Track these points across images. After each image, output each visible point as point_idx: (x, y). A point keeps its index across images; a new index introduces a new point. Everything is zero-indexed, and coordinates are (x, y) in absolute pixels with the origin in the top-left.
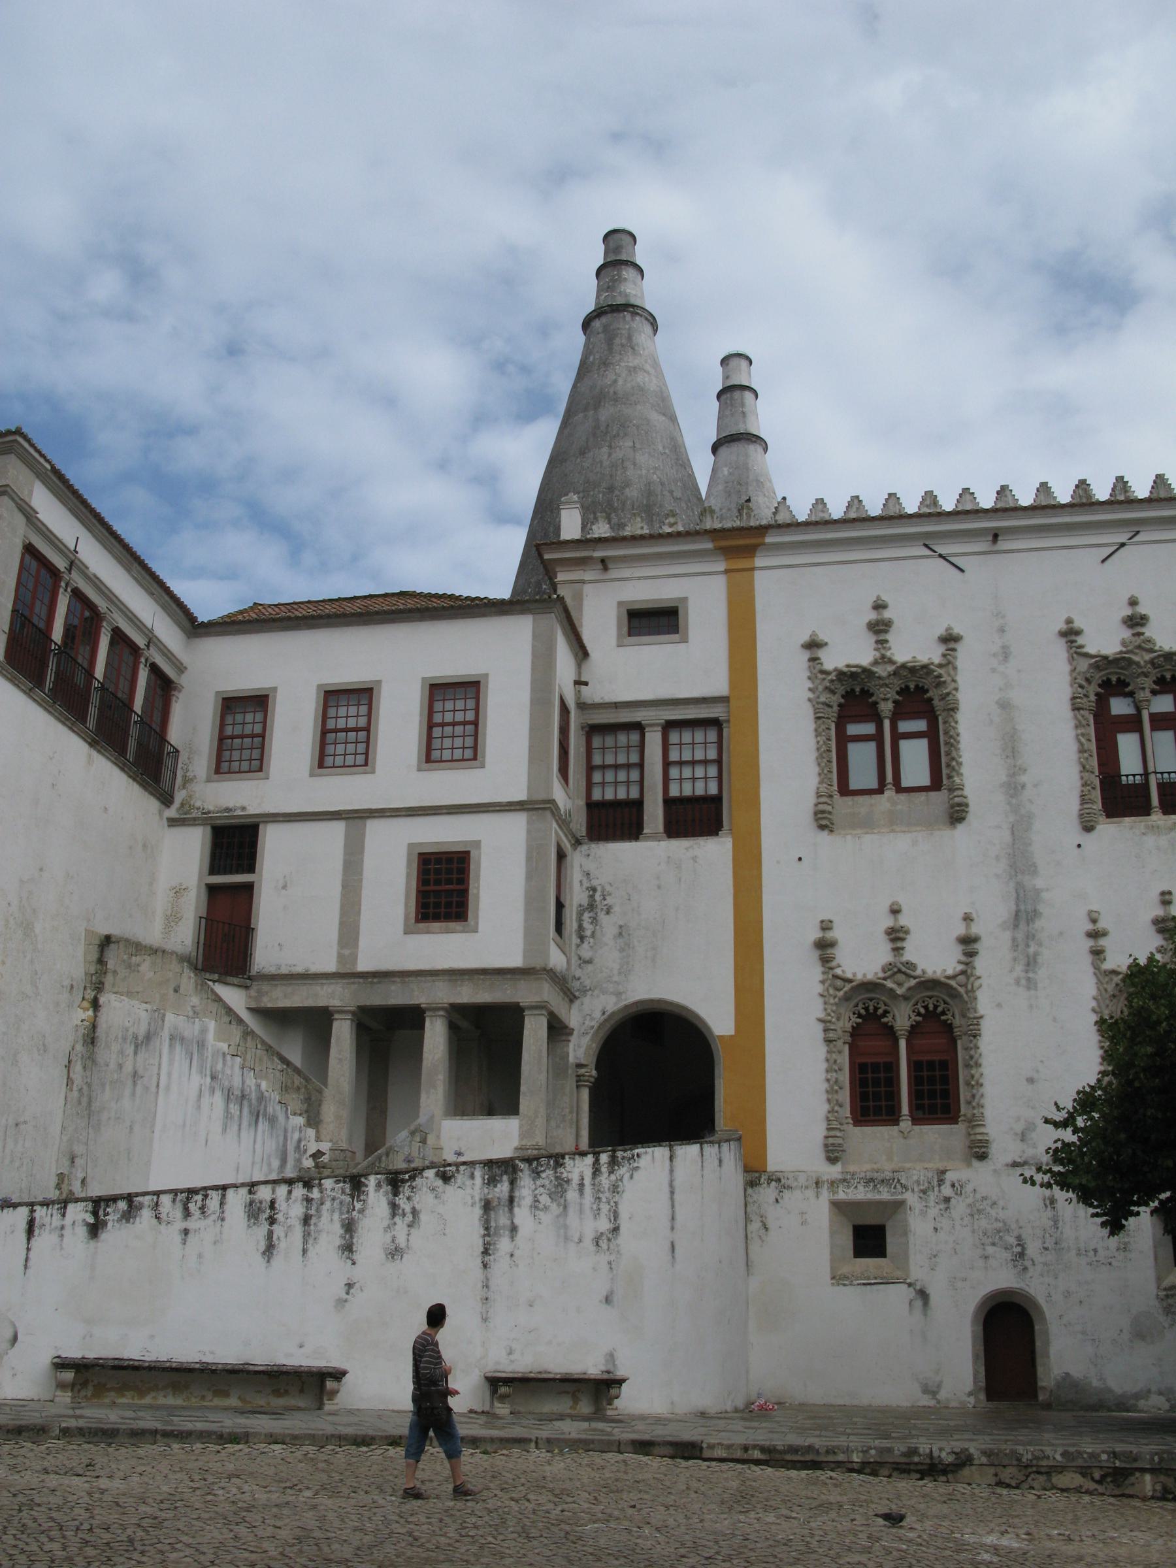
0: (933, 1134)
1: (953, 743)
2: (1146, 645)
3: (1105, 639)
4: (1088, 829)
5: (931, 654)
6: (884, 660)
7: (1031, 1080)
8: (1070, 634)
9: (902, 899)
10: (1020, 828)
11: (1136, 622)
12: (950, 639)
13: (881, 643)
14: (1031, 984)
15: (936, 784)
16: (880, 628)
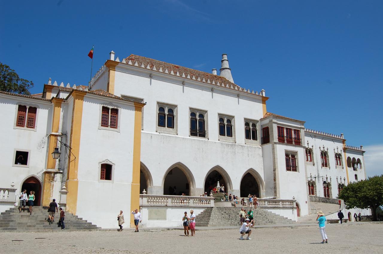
0: (313, 196)
1: (313, 157)
2: (324, 150)
3: (322, 149)
4: (322, 168)
5: (311, 148)
6: (309, 147)
7: (319, 192)
8: (320, 148)
9: (331, 176)
10: (318, 168)
11: (324, 148)
12: (313, 146)
13: (308, 145)
14: (319, 182)
15: (311, 161)
16: (308, 144)
